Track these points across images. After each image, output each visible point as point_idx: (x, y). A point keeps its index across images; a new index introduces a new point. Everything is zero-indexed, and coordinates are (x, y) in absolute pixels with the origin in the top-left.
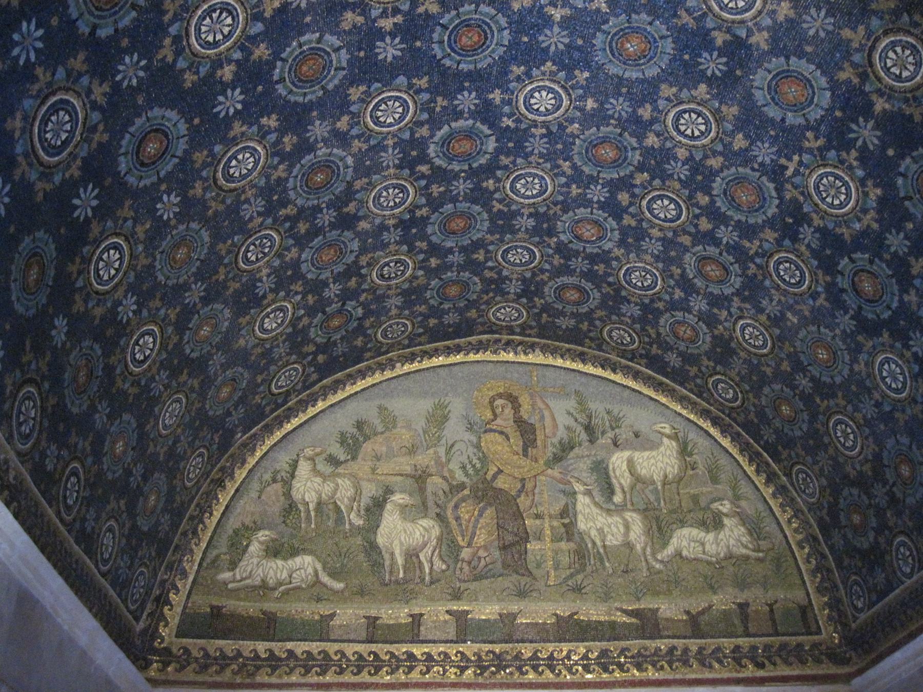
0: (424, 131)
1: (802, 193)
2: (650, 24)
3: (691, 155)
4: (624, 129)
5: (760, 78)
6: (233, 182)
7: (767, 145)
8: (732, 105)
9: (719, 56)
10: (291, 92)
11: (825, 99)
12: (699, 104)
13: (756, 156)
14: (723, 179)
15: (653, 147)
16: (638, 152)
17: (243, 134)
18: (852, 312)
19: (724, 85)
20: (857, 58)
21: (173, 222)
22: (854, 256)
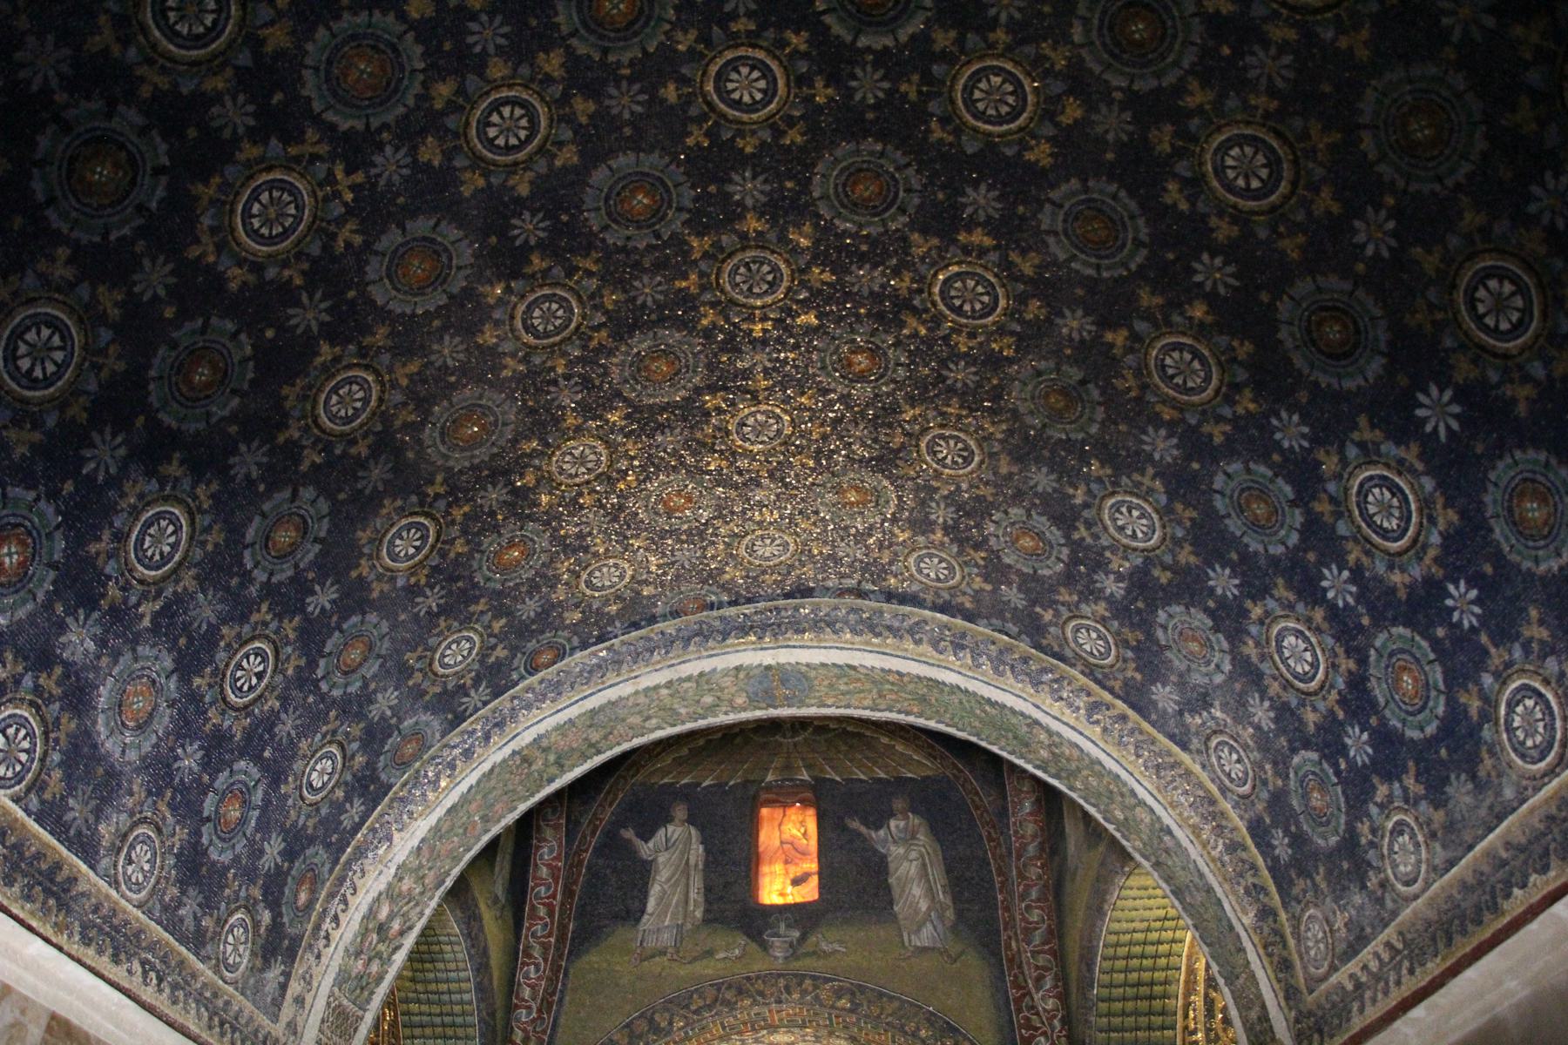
0: (943, 39)
1: (297, 159)
2: (628, 238)
3: (481, 75)
4: (603, 63)
5: (465, 253)
6: (1273, 150)
7: (396, 178)
8: (473, 196)
9: (526, 241)
10: (1132, 217)
11: (378, 294)
12: (516, 164)
13: (397, 149)
14: (414, 71)
15: (547, 52)
16: (565, 30)
17: (1220, 215)
18: (61, 97)
19: (497, 212)
20: (386, 358)
21: (1390, 201)
22: (164, 180)
